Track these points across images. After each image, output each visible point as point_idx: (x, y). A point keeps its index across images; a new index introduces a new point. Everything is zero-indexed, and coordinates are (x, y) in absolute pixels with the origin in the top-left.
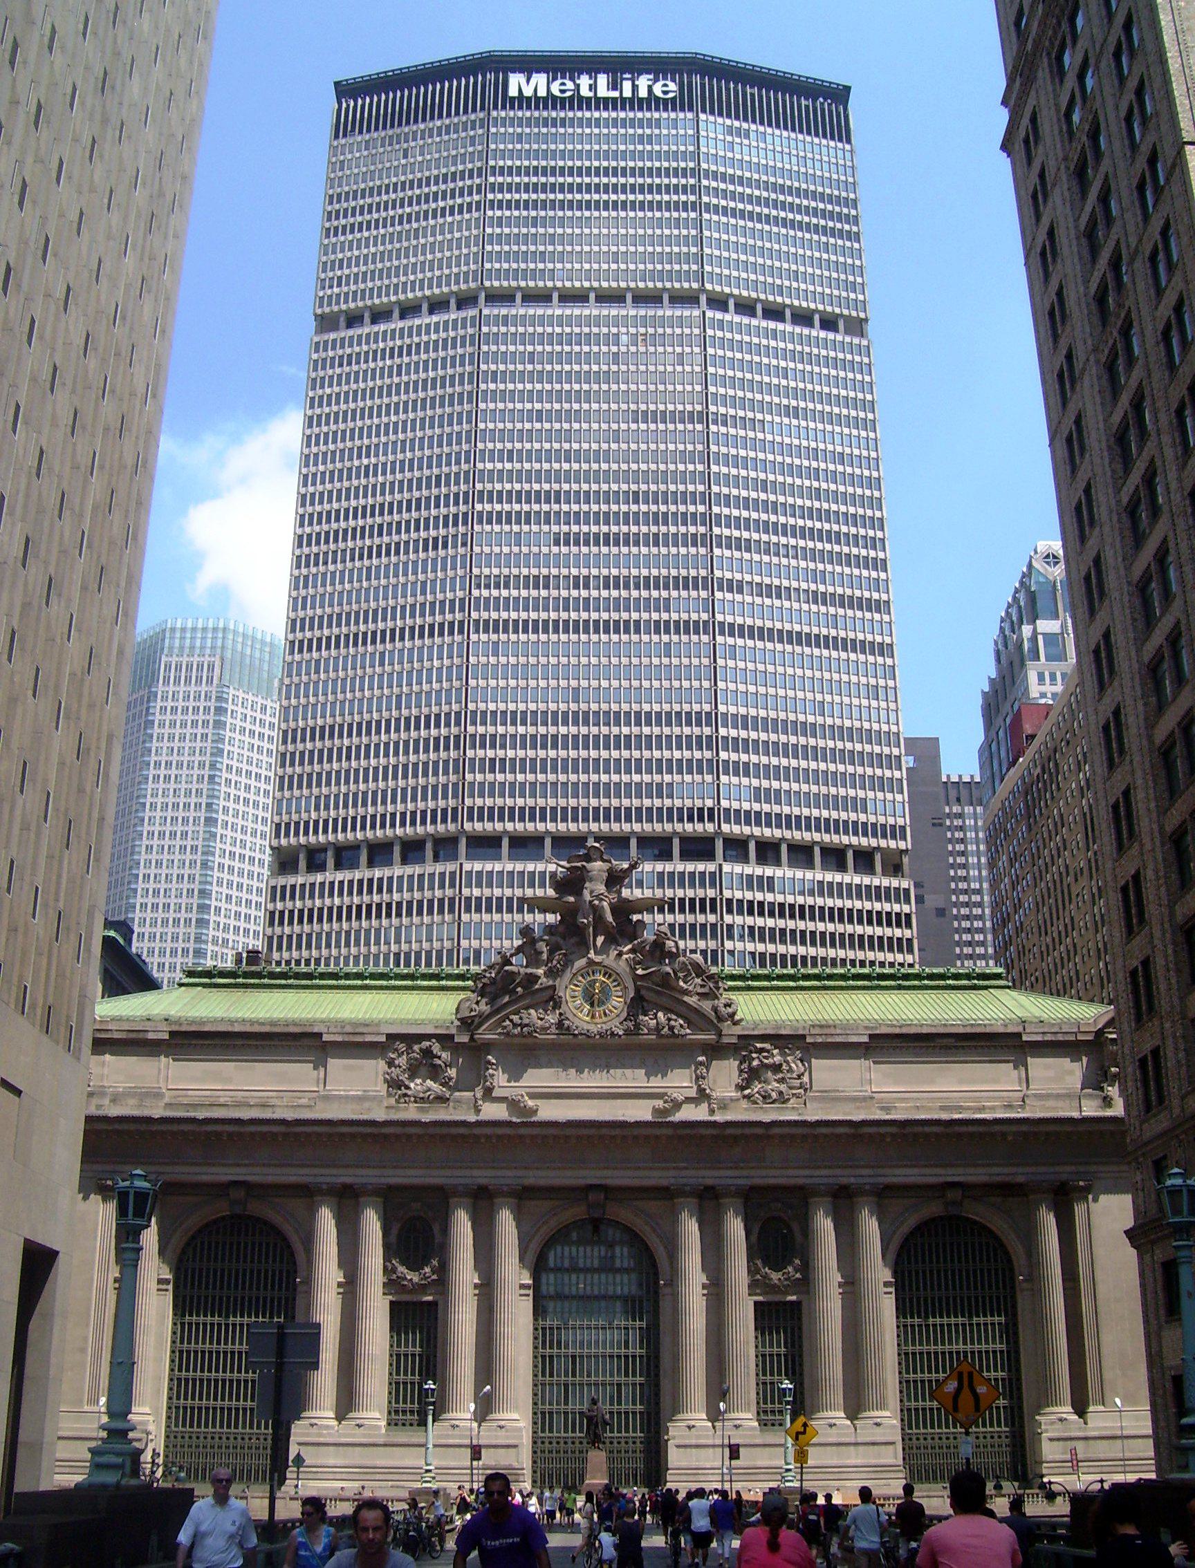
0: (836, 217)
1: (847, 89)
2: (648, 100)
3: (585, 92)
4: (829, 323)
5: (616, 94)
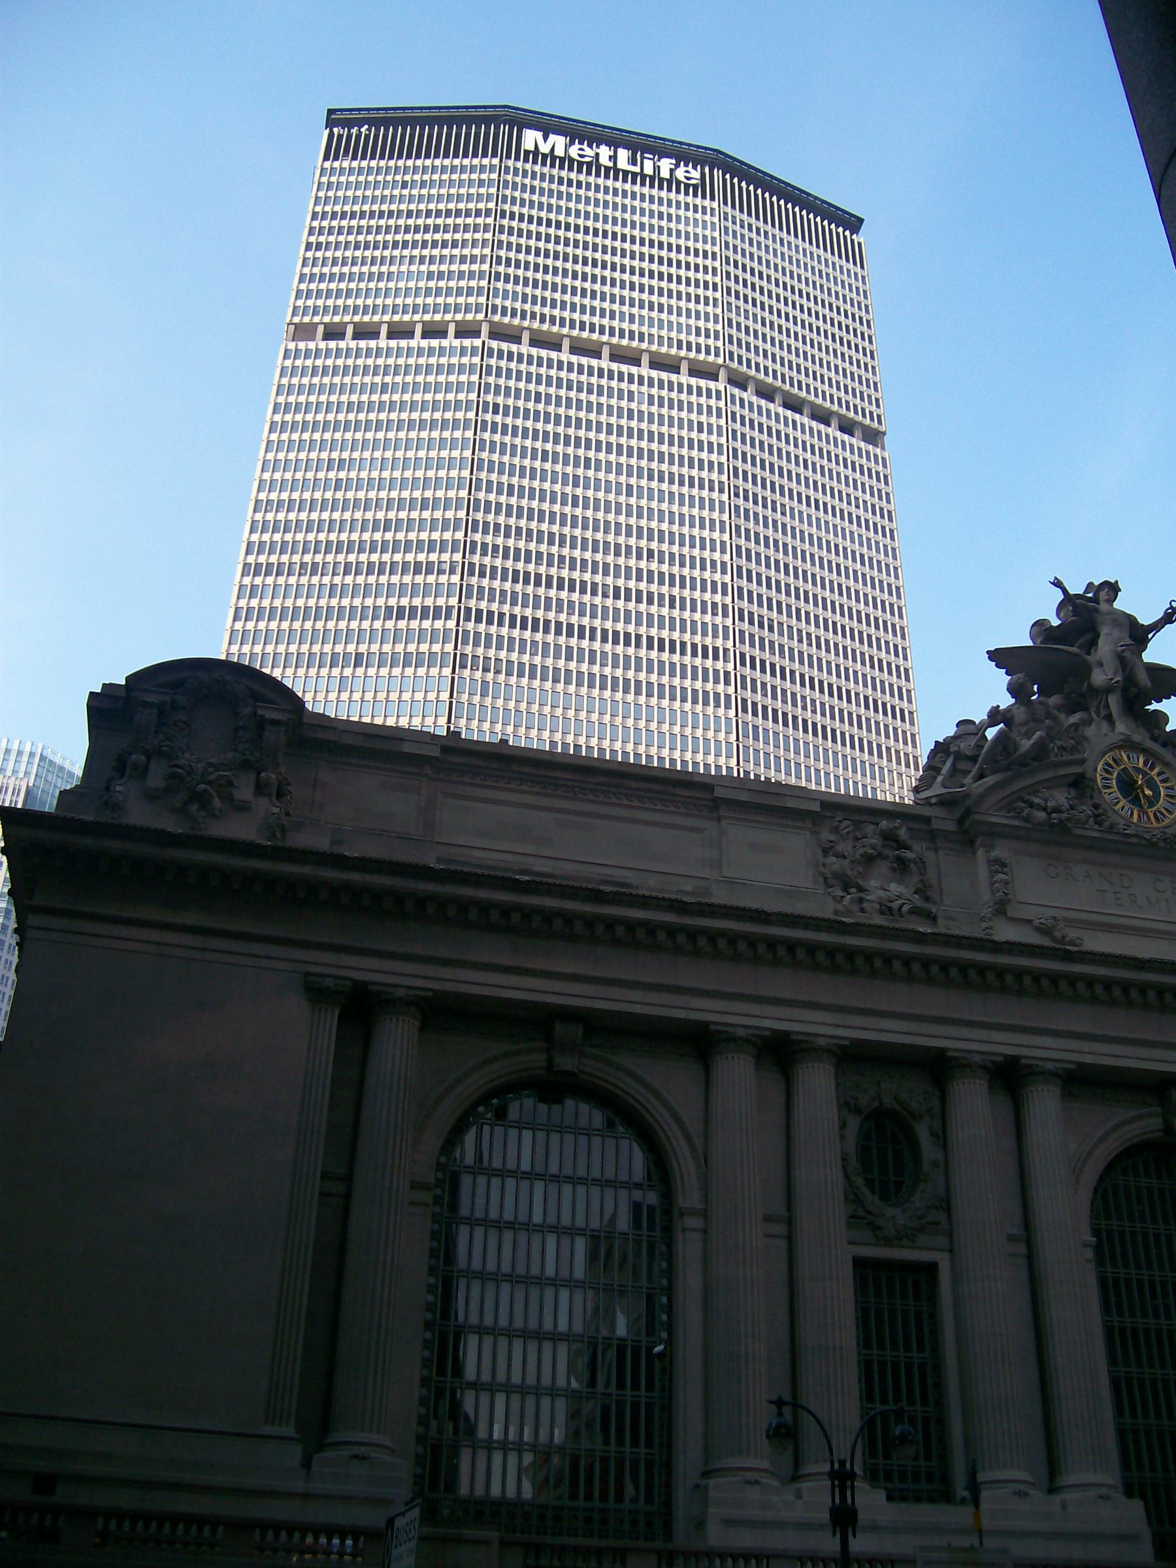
0: (854, 331)
1: (861, 221)
3: (604, 160)
4: (847, 427)
5: (637, 169)
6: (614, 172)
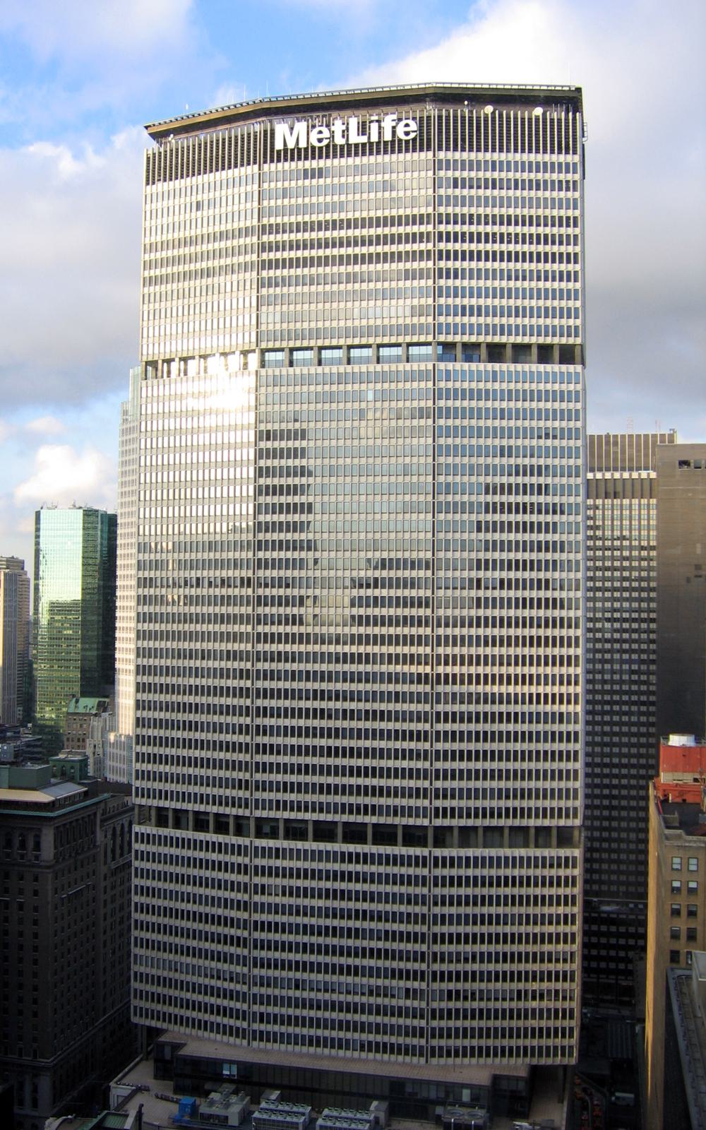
1: (579, 90)
2: (393, 142)
3: (339, 140)
5: (364, 139)
6: (349, 150)
